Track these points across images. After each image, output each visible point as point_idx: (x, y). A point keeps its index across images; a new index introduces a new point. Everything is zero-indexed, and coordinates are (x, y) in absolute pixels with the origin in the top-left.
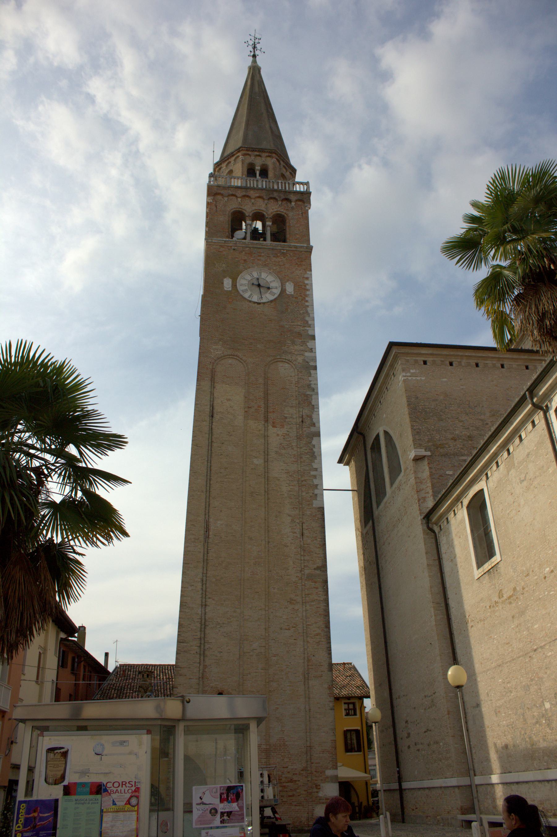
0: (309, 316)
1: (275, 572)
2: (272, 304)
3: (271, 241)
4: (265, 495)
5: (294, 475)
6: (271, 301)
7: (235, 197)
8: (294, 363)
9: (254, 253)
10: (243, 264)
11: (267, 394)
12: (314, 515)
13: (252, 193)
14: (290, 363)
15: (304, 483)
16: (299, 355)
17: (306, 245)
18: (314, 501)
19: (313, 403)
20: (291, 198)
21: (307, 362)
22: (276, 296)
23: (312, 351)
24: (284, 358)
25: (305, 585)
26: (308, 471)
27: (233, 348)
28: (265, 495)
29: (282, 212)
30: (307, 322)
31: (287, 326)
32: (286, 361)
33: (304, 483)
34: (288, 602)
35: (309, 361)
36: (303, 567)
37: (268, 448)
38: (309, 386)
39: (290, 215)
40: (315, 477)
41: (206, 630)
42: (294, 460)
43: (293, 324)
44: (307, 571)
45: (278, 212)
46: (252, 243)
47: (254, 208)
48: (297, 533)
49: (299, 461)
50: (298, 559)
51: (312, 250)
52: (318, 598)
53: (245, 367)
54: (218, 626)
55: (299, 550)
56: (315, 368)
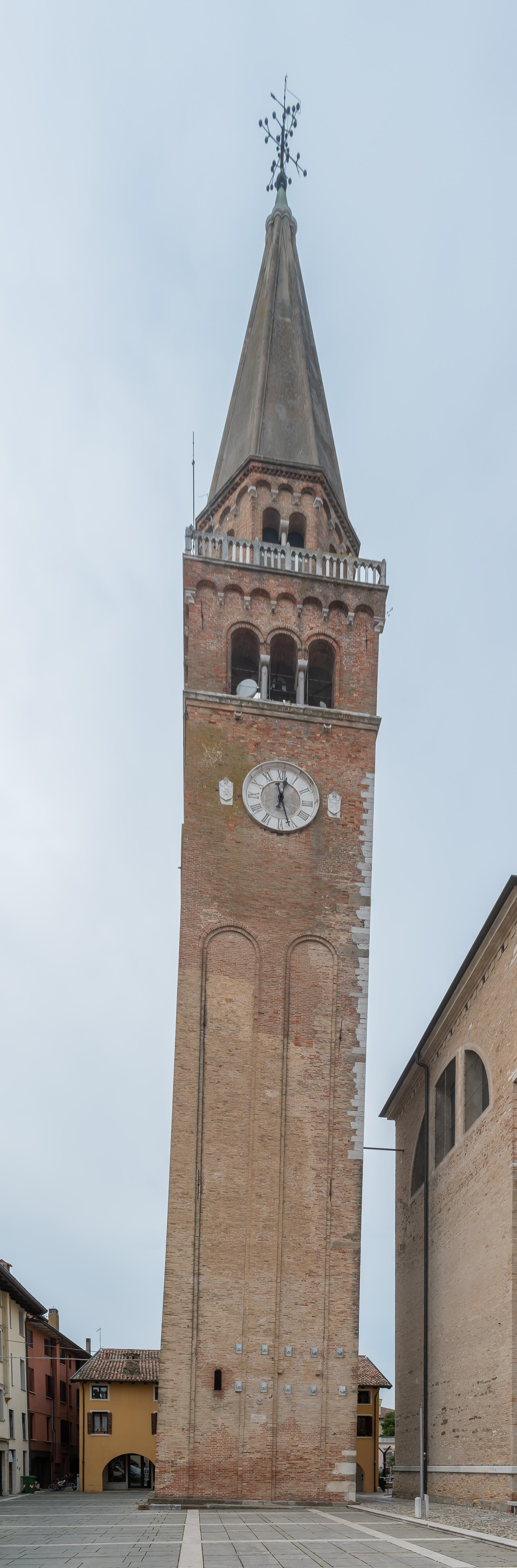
0: (364, 861)
1: (291, 1239)
2: (303, 835)
3: (305, 703)
4: (281, 1140)
5: (324, 1116)
6: (301, 830)
7: (237, 595)
8: (333, 944)
9: (274, 729)
10: (254, 751)
11: (289, 994)
12: (348, 1169)
13: (274, 586)
15: (337, 1126)
16: (342, 930)
17: (368, 715)
18: (349, 1151)
19: (359, 1011)
20: (347, 602)
21: (355, 944)
22: (309, 820)
23: (364, 925)
24: (318, 934)
26: (344, 1111)
27: (236, 915)
28: (281, 1140)
29: (329, 637)
30: (360, 872)
31: (326, 879)
32: (321, 940)
33: (337, 1126)
34: (306, 1274)
35: (357, 942)
36: (328, 1234)
37: (287, 1076)
38: (354, 983)
39: (343, 644)
40: (353, 1118)
42: (325, 1094)
43: (335, 875)
44: (333, 1239)
45: (322, 637)
46: (271, 705)
47: (275, 624)
48: (324, 1192)
49: (332, 1096)
50: (322, 1224)
51: (378, 725)
52: (346, 1271)
53: (255, 948)
55: (325, 1213)
56: (366, 954)
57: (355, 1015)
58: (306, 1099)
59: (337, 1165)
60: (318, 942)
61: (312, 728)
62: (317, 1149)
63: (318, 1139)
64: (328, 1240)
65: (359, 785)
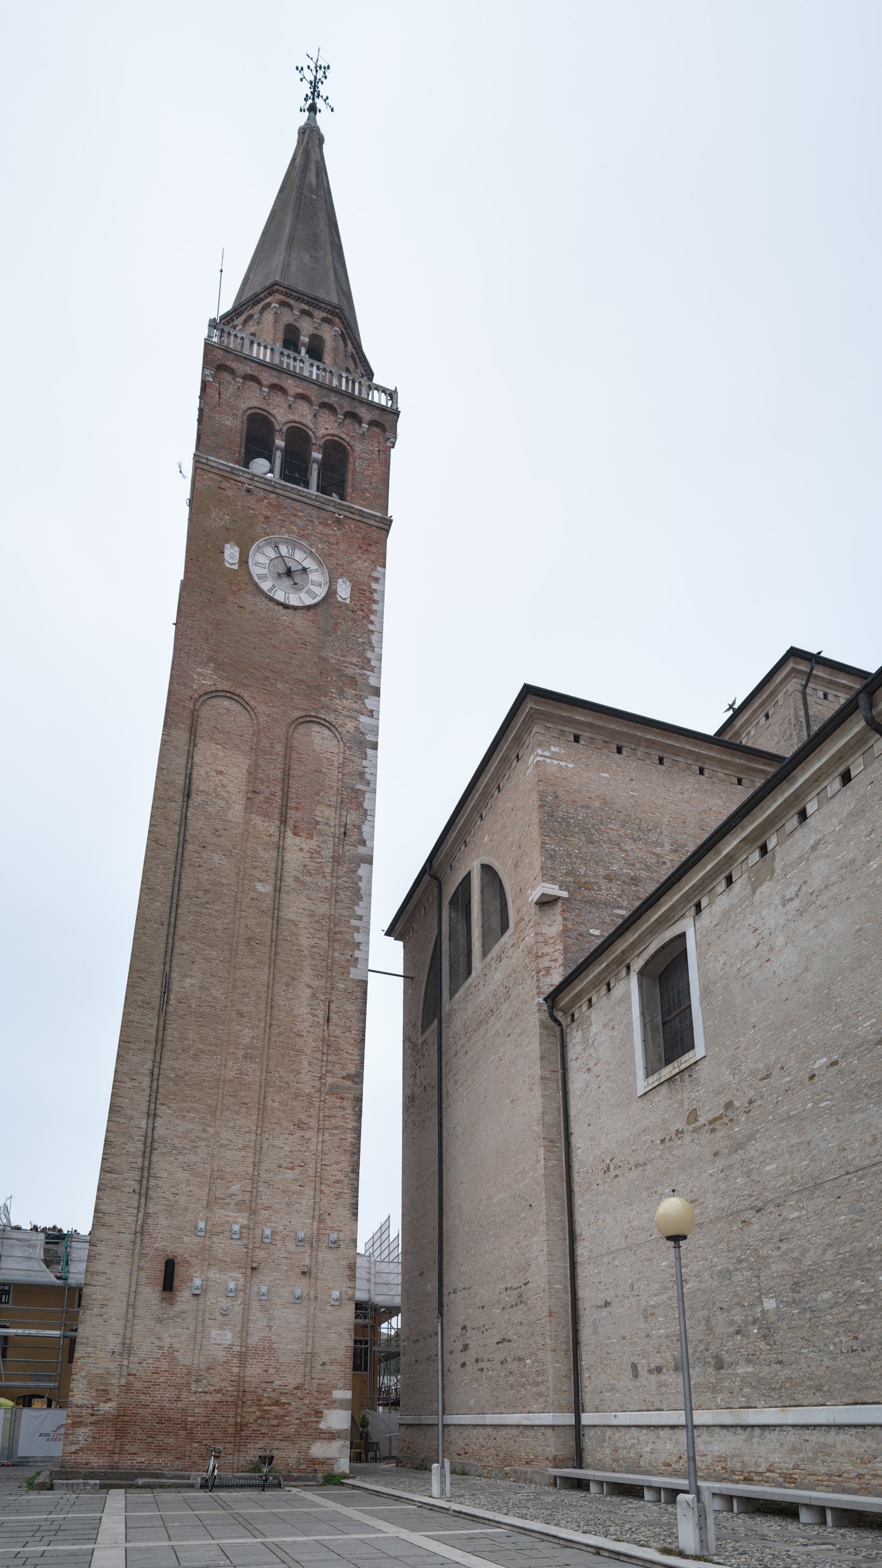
0: (373, 651)
30: (369, 660)
58: (304, 899)
60: (323, 725)
63: (315, 950)
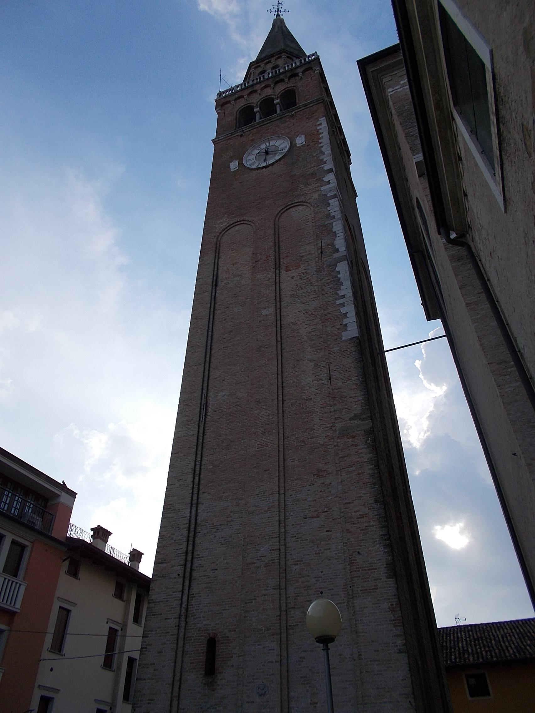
1: (294, 438)
5: (316, 313)
14: (305, 204)
25: (337, 445)
26: (333, 302)
32: (300, 204)
34: (314, 475)
35: (326, 193)
41: (197, 539)
42: (315, 296)
44: (339, 425)
52: (359, 459)
54: (215, 530)
57: (332, 234)
59: (332, 350)
60: (298, 205)
61: (283, 119)
62: (313, 342)
64: (334, 428)
65: (315, 125)
